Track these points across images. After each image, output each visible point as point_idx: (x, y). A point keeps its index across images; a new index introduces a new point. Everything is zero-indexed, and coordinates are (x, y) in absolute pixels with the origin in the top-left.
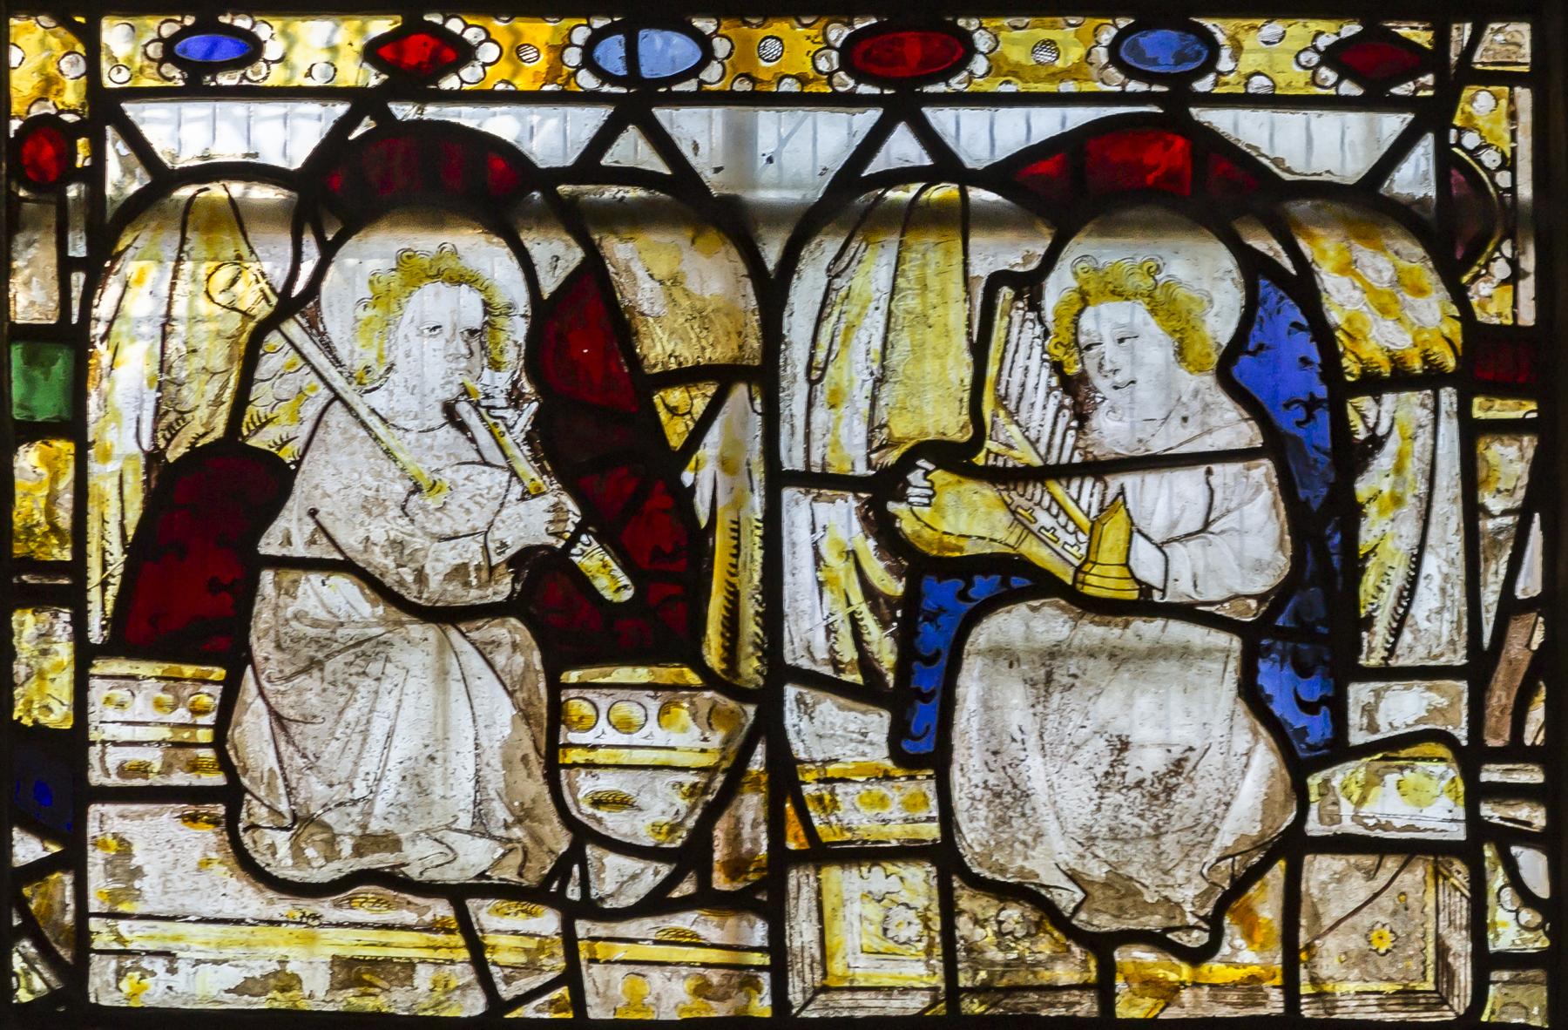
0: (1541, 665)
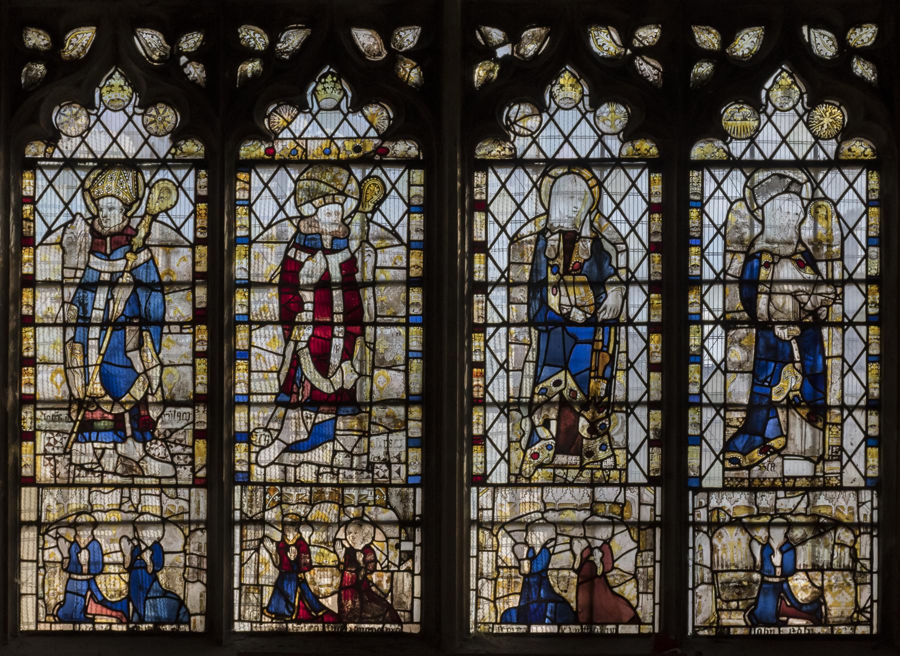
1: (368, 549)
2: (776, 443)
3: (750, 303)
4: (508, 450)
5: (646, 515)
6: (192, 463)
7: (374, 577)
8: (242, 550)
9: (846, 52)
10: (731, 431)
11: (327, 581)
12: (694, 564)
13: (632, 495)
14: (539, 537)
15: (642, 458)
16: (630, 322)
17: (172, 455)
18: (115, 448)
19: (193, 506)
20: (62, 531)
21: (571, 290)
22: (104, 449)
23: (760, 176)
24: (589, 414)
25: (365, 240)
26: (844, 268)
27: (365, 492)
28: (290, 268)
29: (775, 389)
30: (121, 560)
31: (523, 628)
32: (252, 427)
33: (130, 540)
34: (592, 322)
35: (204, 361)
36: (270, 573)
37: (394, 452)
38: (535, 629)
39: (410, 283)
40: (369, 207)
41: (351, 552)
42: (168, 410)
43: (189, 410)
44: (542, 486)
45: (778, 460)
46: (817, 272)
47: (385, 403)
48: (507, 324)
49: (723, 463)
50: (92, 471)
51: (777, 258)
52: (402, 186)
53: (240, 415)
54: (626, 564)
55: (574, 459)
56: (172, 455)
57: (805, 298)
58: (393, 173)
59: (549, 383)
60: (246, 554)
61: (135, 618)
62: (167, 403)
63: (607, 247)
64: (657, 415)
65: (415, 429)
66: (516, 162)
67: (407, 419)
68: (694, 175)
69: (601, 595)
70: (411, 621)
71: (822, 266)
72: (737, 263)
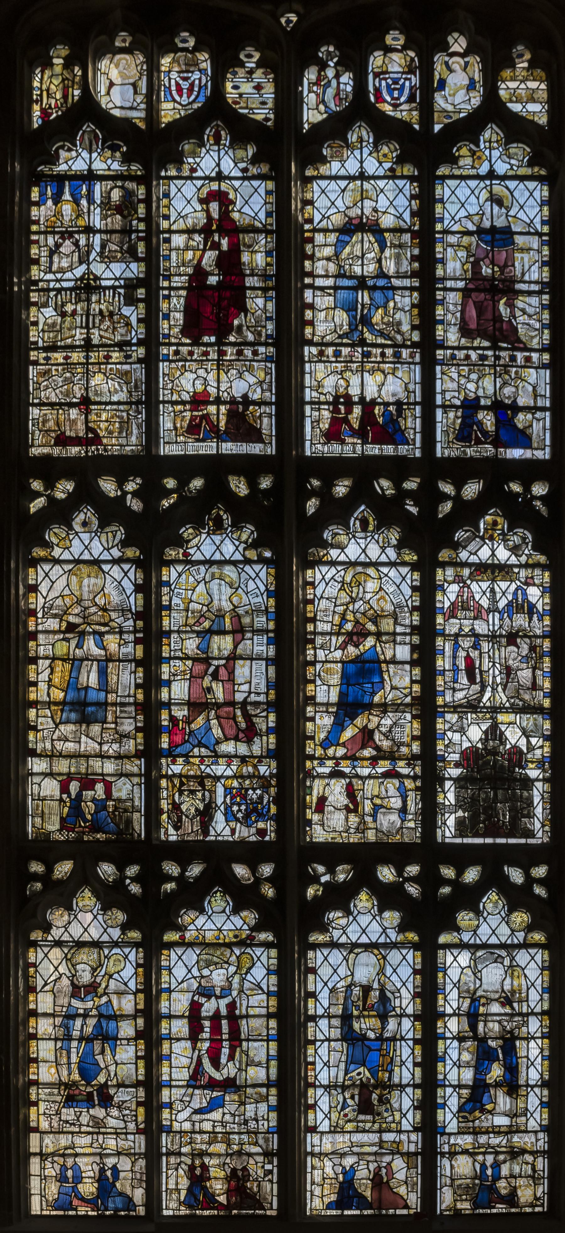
0: (421, 814)
1: (245, 1169)
2: (489, 1107)
3: (473, 1027)
4: (330, 1112)
5: (412, 1148)
6: (136, 1120)
7: (249, 1185)
8: (167, 1169)
9: (530, 880)
10: (463, 1100)
11: (219, 1187)
12: (441, 1175)
13: (404, 1137)
14: (349, 1161)
15: (410, 1116)
16: (402, 1039)
17: (124, 1116)
18: (88, 1112)
19: (137, 1145)
20: (56, 1159)
21: (367, 1020)
22: (81, 1112)
23: (479, 953)
24: (378, 1092)
25: (241, 991)
26: (528, 1006)
27: (242, 1137)
28: (195, 1007)
29: (488, 1076)
30: (93, 1175)
31: (339, 1212)
32: (173, 1100)
33: (98, 1164)
34: (380, 1039)
35: (142, 1061)
36: (184, 1183)
37: (260, 1114)
38: (346, 1212)
39: (269, 1016)
40: (244, 971)
41: (234, 1171)
42: (120, 1089)
43: (134, 1090)
44: (350, 1132)
45: (490, 1117)
46: (513, 1008)
47: (254, 1086)
48: (329, 1040)
49: (458, 1118)
50: (74, 1124)
51: (489, 1001)
52: (264, 959)
53: (165, 1092)
54: (401, 1176)
55: (369, 1117)
56: (124, 1116)
57: (506, 1024)
58: (258, 951)
59: (354, 1074)
60: (170, 1172)
61: (102, 1208)
62: (119, 1086)
63: (389, 995)
64: (419, 1092)
65: (273, 1100)
66: (333, 945)
67: (268, 1095)
68: (441, 953)
69: (385, 1193)
70: (271, 1209)
71: (515, 1005)
72: (466, 1003)
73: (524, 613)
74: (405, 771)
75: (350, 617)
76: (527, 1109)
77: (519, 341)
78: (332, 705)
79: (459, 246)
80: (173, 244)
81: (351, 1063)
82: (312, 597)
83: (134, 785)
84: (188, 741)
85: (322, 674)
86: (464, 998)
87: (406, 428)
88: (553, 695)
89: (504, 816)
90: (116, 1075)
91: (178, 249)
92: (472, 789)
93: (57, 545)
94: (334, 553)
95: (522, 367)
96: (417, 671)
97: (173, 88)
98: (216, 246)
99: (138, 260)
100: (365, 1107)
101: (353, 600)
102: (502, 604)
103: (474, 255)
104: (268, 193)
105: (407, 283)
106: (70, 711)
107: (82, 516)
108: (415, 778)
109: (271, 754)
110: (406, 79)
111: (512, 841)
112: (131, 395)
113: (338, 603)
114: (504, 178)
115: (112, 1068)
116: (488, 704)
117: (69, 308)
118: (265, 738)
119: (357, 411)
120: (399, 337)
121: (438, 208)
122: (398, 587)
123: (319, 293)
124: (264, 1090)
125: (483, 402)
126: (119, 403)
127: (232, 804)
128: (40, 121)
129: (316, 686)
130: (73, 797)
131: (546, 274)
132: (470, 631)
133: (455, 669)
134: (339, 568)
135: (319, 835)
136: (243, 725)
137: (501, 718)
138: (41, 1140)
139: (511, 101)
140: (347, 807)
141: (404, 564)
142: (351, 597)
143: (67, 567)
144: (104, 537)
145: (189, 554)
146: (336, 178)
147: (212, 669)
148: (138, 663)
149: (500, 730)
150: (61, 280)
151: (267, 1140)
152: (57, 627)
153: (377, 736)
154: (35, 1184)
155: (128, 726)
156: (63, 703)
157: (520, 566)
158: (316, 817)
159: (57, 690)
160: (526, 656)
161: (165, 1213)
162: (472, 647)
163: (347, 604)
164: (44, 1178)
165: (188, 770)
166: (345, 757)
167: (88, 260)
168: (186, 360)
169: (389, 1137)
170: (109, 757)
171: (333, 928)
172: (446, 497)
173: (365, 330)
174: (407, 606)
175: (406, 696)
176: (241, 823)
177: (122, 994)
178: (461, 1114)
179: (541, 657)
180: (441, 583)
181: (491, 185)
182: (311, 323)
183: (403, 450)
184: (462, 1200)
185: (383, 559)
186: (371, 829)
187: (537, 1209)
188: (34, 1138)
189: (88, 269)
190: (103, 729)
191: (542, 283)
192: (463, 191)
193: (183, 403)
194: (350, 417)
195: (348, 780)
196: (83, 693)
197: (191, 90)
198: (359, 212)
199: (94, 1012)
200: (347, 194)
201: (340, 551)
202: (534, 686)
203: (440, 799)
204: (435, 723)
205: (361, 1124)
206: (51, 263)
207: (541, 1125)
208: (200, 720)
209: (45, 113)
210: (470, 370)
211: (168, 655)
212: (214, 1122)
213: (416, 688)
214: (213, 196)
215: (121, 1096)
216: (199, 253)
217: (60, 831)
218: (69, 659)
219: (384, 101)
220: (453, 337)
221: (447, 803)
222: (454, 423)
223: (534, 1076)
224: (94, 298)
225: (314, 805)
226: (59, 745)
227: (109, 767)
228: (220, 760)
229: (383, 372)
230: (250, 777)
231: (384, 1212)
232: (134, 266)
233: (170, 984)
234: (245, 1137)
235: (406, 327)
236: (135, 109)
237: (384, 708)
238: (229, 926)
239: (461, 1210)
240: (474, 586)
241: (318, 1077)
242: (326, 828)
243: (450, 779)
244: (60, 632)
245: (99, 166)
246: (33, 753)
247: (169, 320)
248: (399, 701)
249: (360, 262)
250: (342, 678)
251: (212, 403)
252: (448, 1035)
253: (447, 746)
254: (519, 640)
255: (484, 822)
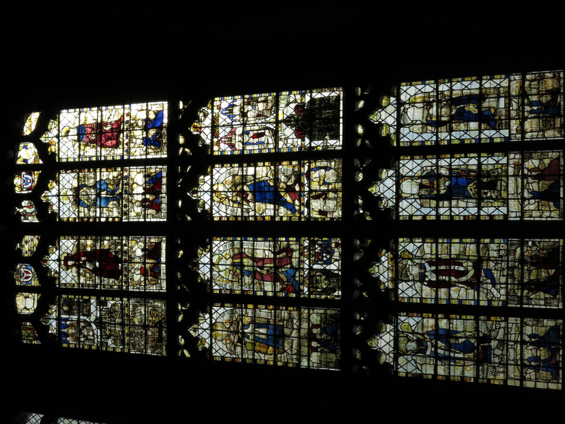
3: (444, 123)
6: (499, 322)
8: (531, 304)
12: (537, 138)
13: (511, 162)
22: (494, 354)
26: (432, 92)
27: (510, 259)
28: (431, 284)
31: (562, 201)
33: (528, 346)
37: (496, 248)
38: (562, 196)
44: (508, 194)
46: (433, 101)
48: (450, 208)
50: (501, 359)
54: (536, 163)
55: (499, 183)
56: (496, 329)
59: (471, 192)
60: (533, 303)
63: (424, 174)
64: (482, 155)
65: (487, 241)
68: (401, 144)
70: (559, 242)
73: (233, 109)
74: (306, 168)
75: (234, 199)
76: (495, 88)
77: (120, 120)
78: (275, 207)
79: (84, 150)
80: (84, 282)
81: (464, 194)
82: (226, 218)
83: (314, 313)
84: (292, 283)
85: (260, 213)
86: (427, 130)
87: (155, 173)
88: (270, 92)
89: (329, 113)
90: (471, 332)
91: (86, 281)
92: (315, 131)
93: (204, 345)
94: (207, 207)
95: (130, 118)
96: (260, 164)
97: (26, 280)
98: (84, 262)
99: (90, 299)
100: (492, 186)
101: (227, 197)
102: (230, 121)
103: (88, 143)
104: (65, 239)
105: (98, 174)
106: (278, 344)
107: (191, 332)
108: (310, 163)
109: (298, 239)
110: (23, 177)
111: (341, 108)
112: (142, 305)
113: (228, 205)
114: (59, 130)
115: (468, 334)
116: (274, 125)
117: (108, 332)
118: (291, 243)
119: (148, 196)
120: (119, 177)
121: (71, 160)
122: (221, 174)
123: (102, 215)
124: (481, 246)
125: (145, 136)
126: (145, 311)
127: (322, 260)
128: (38, 341)
129: (266, 216)
130: (319, 345)
131: (96, 109)
132: (241, 136)
133: (258, 143)
134: (213, 204)
135: (338, 214)
136: (284, 254)
137: (280, 118)
138: (511, 379)
139: (31, 129)
140: (324, 199)
141: (212, 172)
142: (226, 198)
143: (214, 341)
144: (201, 322)
145: (208, 279)
146: (59, 207)
147: (258, 270)
148: (255, 307)
149: (286, 118)
150: (97, 335)
151: (512, 245)
152: (240, 348)
153: (289, 184)
154: (540, 385)
155: (285, 314)
156: (274, 347)
157: (212, 112)
158: (329, 216)
159: (269, 351)
160: (252, 106)
161: (561, 307)
162: (248, 135)
163: (229, 200)
164: (537, 380)
165: (306, 283)
166: (300, 201)
167: (89, 322)
168: (128, 278)
169: (511, 171)
170: (300, 325)
171: (387, 205)
172: (183, 150)
173: (116, 193)
174: (230, 169)
175: (270, 169)
176: (333, 256)
177: (423, 325)
178: (497, 128)
179: (252, 98)
180: (220, 152)
181: (62, 136)
182: (114, 218)
183: (164, 174)
184: (554, 124)
185: (209, 182)
186: (335, 186)
187: (562, 75)
188: (510, 383)
189: (93, 322)
190: (286, 327)
191: (98, 110)
192: (63, 149)
193: (145, 280)
194: (151, 200)
195: (311, 199)
196: (270, 337)
197: (27, 273)
198: (72, 197)
199: (434, 341)
200: (65, 202)
201: (206, 204)
202: (266, 101)
203: (320, 148)
204: (284, 153)
205: (503, 188)
206: (90, 339)
207: (505, 79)
208: (282, 276)
209: (35, 338)
210: (132, 143)
211: (252, 292)
212: (500, 275)
213: (267, 164)
214: (66, 264)
215: (483, 328)
216: (88, 271)
217: (336, 354)
218: (254, 343)
219: (31, 186)
220: (119, 151)
221: (322, 145)
222: (153, 149)
223: (476, 85)
224: (104, 320)
225: (323, 217)
226: (295, 351)
227: (305, 325)
228: (302, 266)
229: (133, 184)
230: (309, 251)
231: (562, 172)
232: (92, 301)
233: (417, 298)
234: (511, 258)
235: (115, 174)
236: (34, 297)
237: (276, 180)
238: (386, 264)
239: (561, 124)
240: (221, 136)
241: (473, 213)
242: (335, 210)
243: (310, 143)
244: (242, 347)
245: (54, 315)
246: (299, 364)
247: (113, 285)
248: (273, 172)
249: (90, 196)
250: (262, 202)
251: (145, 266)
252: (448, 138)
253: (294, 146)
254: (245, 111)
255: (332, 124)
